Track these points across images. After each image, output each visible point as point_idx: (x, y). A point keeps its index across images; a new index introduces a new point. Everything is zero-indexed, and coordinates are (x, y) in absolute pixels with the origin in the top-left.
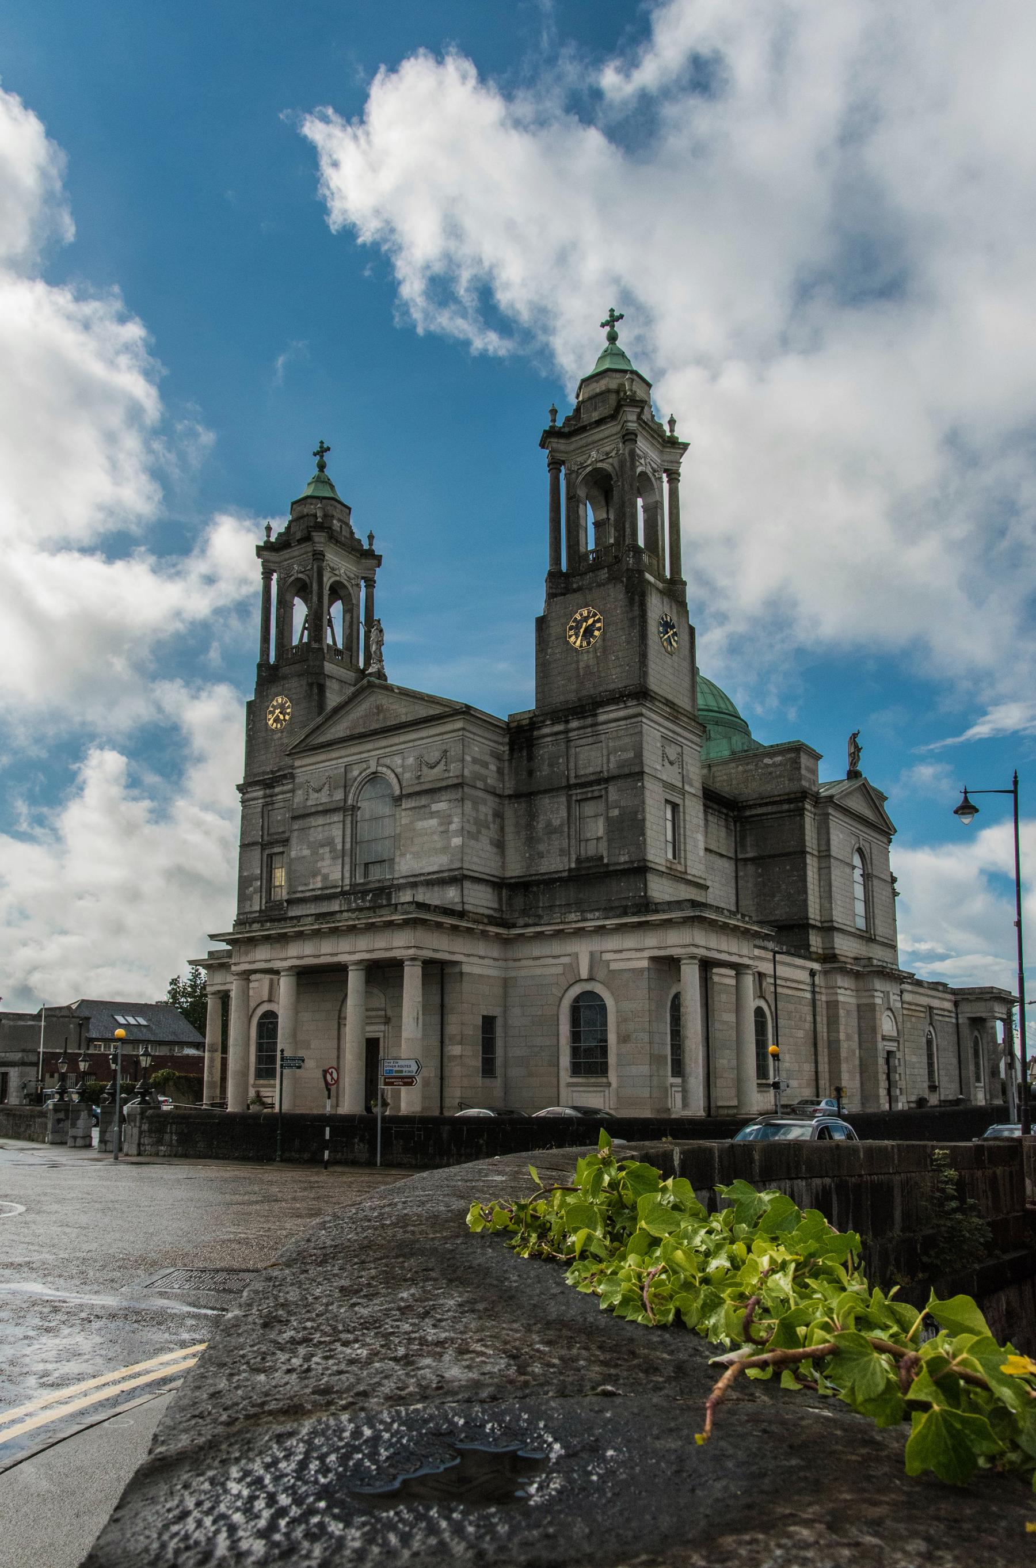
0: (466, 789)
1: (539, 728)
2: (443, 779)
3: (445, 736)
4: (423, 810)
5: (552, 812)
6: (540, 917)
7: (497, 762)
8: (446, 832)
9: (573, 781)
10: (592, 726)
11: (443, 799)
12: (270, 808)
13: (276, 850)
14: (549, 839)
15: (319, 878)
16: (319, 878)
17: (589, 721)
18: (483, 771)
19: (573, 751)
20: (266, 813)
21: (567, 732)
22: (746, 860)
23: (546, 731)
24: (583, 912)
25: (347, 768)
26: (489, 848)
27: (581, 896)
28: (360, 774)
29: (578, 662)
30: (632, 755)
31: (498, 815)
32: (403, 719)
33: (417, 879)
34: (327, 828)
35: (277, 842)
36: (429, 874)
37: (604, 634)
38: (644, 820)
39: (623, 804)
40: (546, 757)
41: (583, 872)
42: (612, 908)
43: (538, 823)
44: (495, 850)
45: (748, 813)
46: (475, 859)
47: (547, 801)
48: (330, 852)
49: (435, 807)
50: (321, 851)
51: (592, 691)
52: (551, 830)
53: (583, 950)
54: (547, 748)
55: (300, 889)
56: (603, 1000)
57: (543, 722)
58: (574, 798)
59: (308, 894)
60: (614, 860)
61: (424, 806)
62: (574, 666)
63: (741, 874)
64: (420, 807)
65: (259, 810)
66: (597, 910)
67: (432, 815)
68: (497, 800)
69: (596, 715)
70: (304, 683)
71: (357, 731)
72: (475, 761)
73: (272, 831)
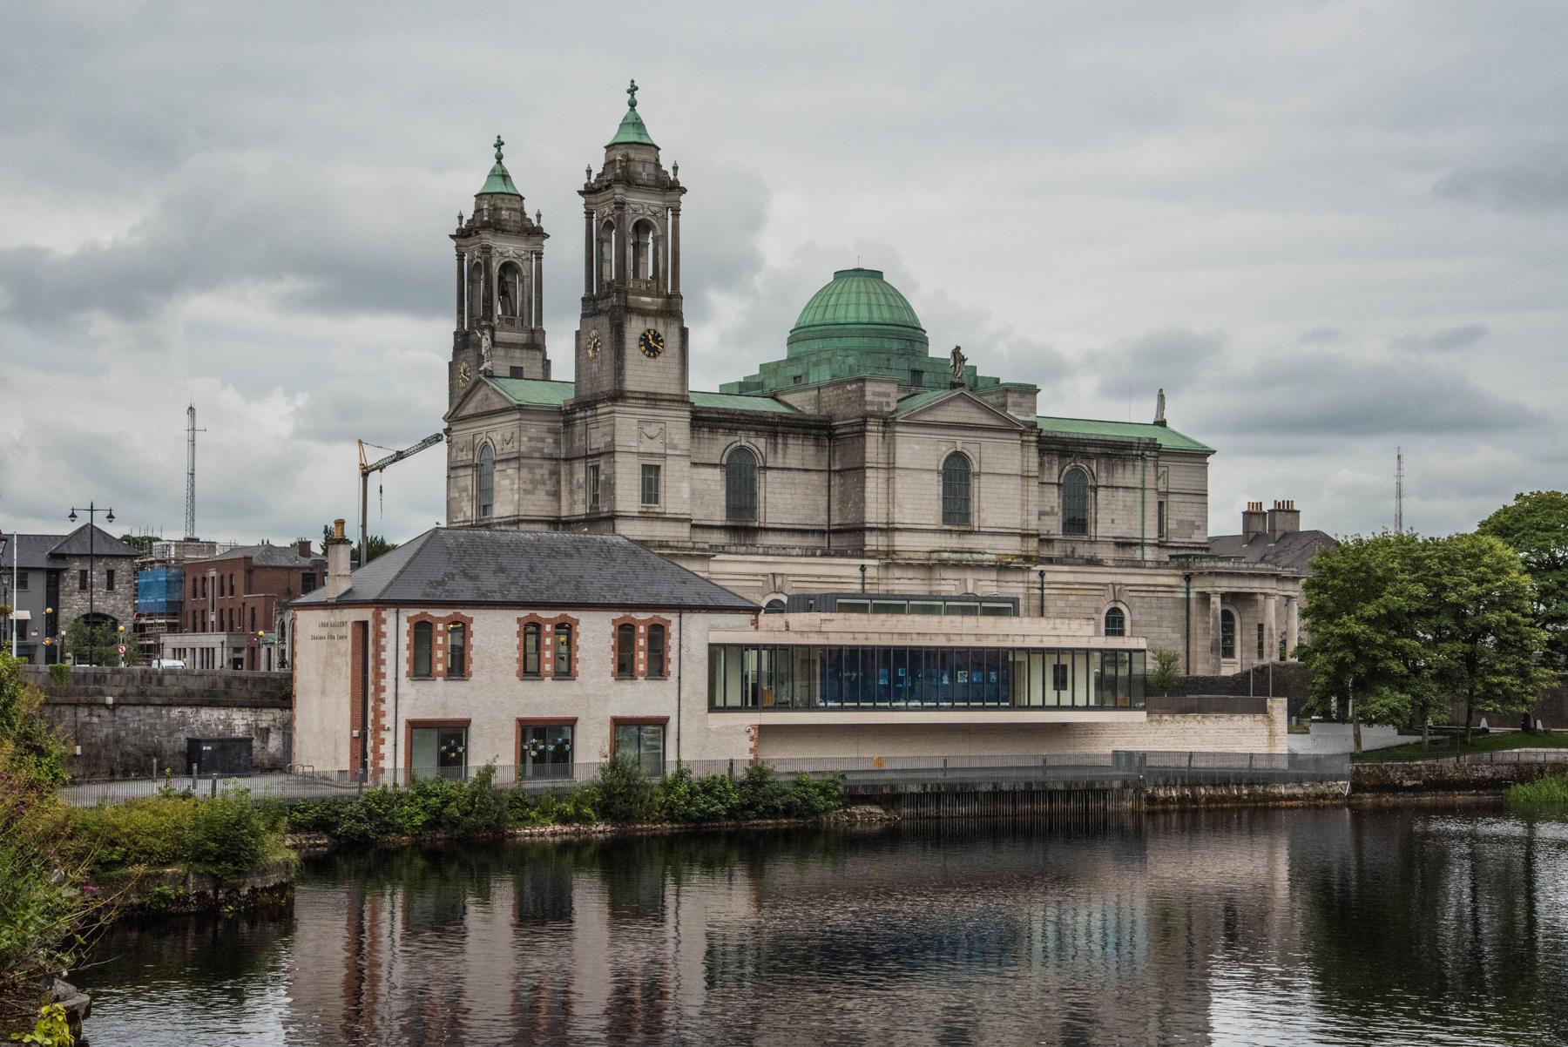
0: (522, 461)
7: (552, 435)
9: (589, 453)
18: (540, 445)
22: (835, 471)
23: (578, 415)
26: (546, 498)
31: (555, 474)
38: (614, 484)
44: (551, 498)
45: (837, 432)
46: (530, 507)
63: (832, 483)
68: (555, 463)
72: (531, 439)
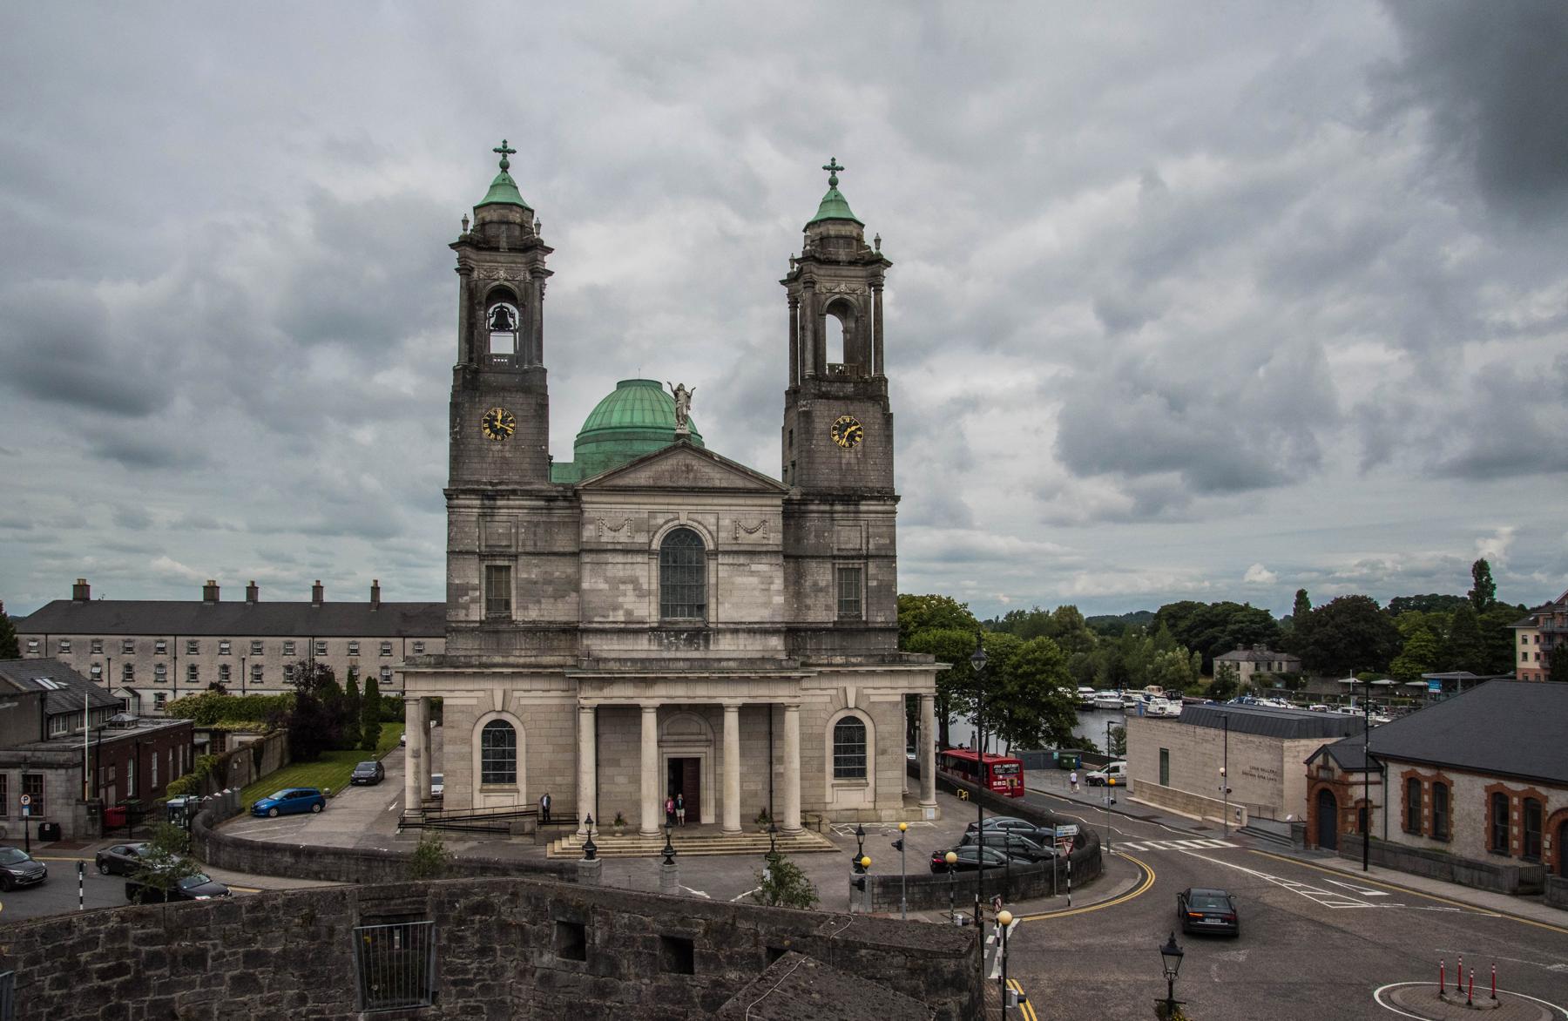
1: (806, 504)
2: (763, 545)
3: (764, 508)
4: (742, 568)
5: (818, 575)
6: (809, 657)
8: (768, 590)
9: (835, 553)
10: (854, 513)
11: (763, 561)
12: (488, 519)
13: (499, 563)
14: (816, 596)
15: (621, 612)
16: (621, 612)
17: (852, 508)
19: (836, 528)
20: (482, 524)
21: (832, 512)
24: (847, 656)
25: (652, 514)
27: (844, 644)
28: (666, 523)
29: (841, 458)
30: (888, 542)
32: (717, 484)
33: (739, 627)
34: (628, 566)
35: (502, 555)
36: (750, 623)
37: (864, 440)
39: (880, 578)
40: (813, 529)
41: (846, 626)
42: (872, 656)
43: (806, 581)
47: (814, 565)
48: (634, 590)
49: (754, 567)
50: (622, 587)
51: (853, 484)
52: (817, 589)
53: (852, 687)
54: (813, 522)
55: (596, 619)
56: (862, 722)
57: (812, 500)
58: (837, 566)
59: (607, 626)
60: (871, 619)
61: (743, 565)
62: (836, 460)
64: (740, 565)
65: (474, 519)
66: (860, 656)
67: (752, 573)
69: (858, 505)
70: (533, 401)
71: (661, 483)
73: (491, 542)
